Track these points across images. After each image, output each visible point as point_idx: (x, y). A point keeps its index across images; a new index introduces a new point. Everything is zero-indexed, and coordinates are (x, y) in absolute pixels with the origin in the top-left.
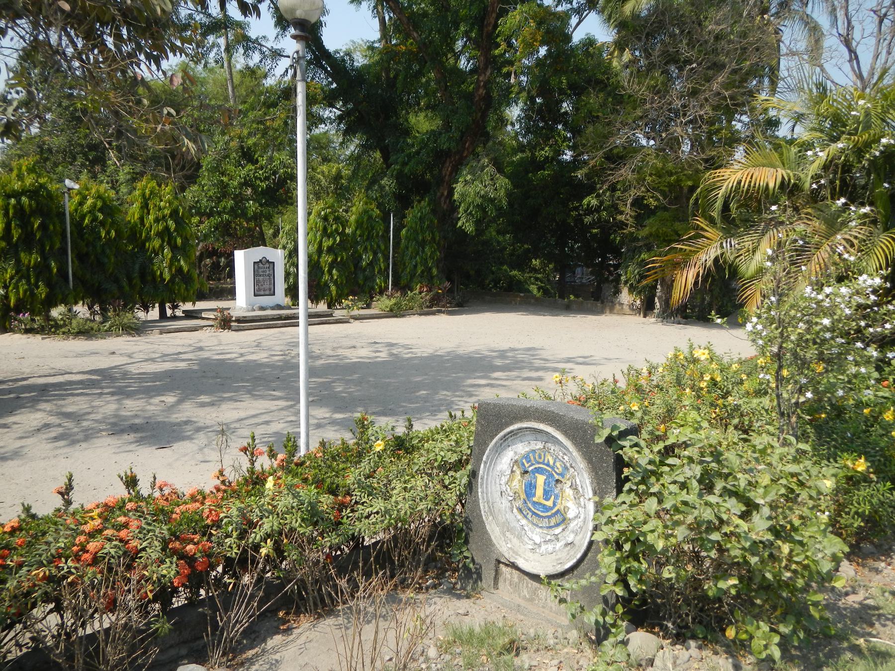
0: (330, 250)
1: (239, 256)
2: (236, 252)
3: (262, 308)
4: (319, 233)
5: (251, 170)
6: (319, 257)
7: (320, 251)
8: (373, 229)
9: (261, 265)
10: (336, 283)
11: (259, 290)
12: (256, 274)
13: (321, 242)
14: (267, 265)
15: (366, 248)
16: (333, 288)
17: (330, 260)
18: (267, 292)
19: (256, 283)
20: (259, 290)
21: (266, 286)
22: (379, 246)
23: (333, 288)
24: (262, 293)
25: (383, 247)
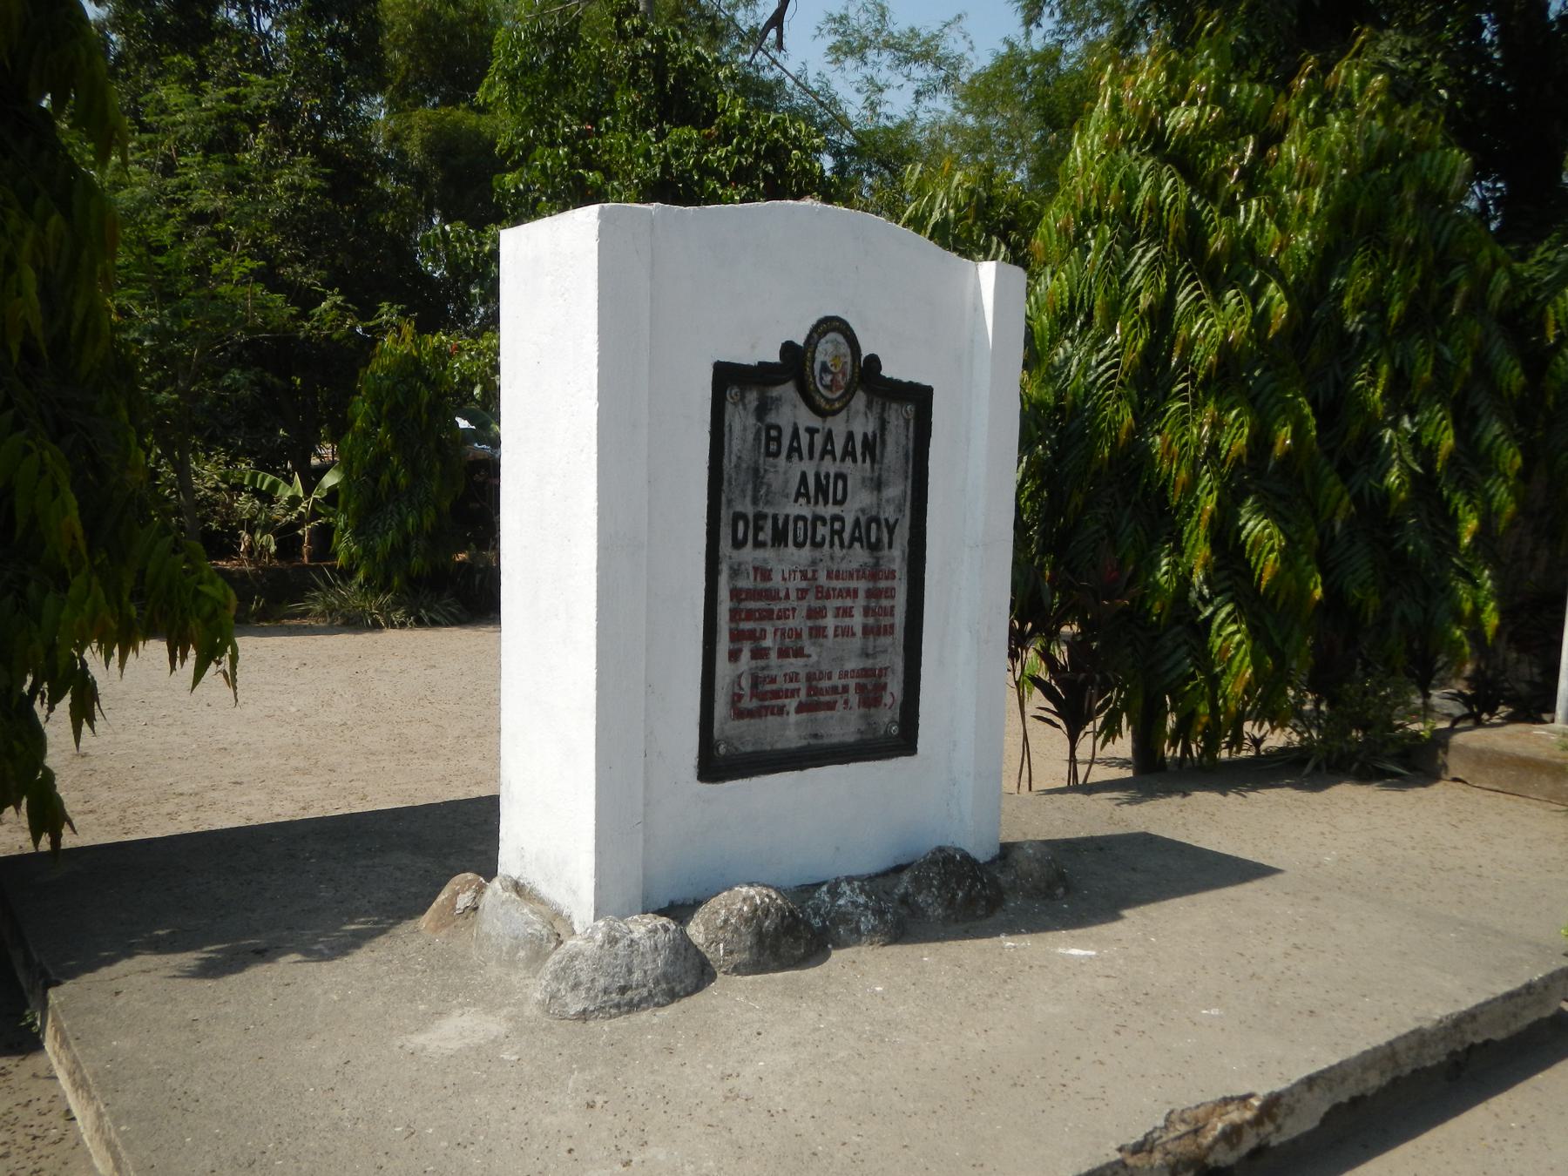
0: (1227, 376)
1: (552, 278)
2: (503, 233)
3: (796, 933)
4: (1143, 256)
5: (688, 142)
6: (1147, 416)
7: (1151, 378)
8: (1443, 265)
9: (792, 413)
10: (1257, 609)
11: (762, 698)
12: (736, 512)
13: (1161, 316)
14: (859, 421)
15: (1399, 386)
16: (1229, 635)
17: (1236, 441)
18: (843, 725)
19: (737, 615)
20: (762, 698)
21: (838, 656)
22: (1484, 369)
23: (1229, 635)
24: (790, 730)
25: (1513, 377)
